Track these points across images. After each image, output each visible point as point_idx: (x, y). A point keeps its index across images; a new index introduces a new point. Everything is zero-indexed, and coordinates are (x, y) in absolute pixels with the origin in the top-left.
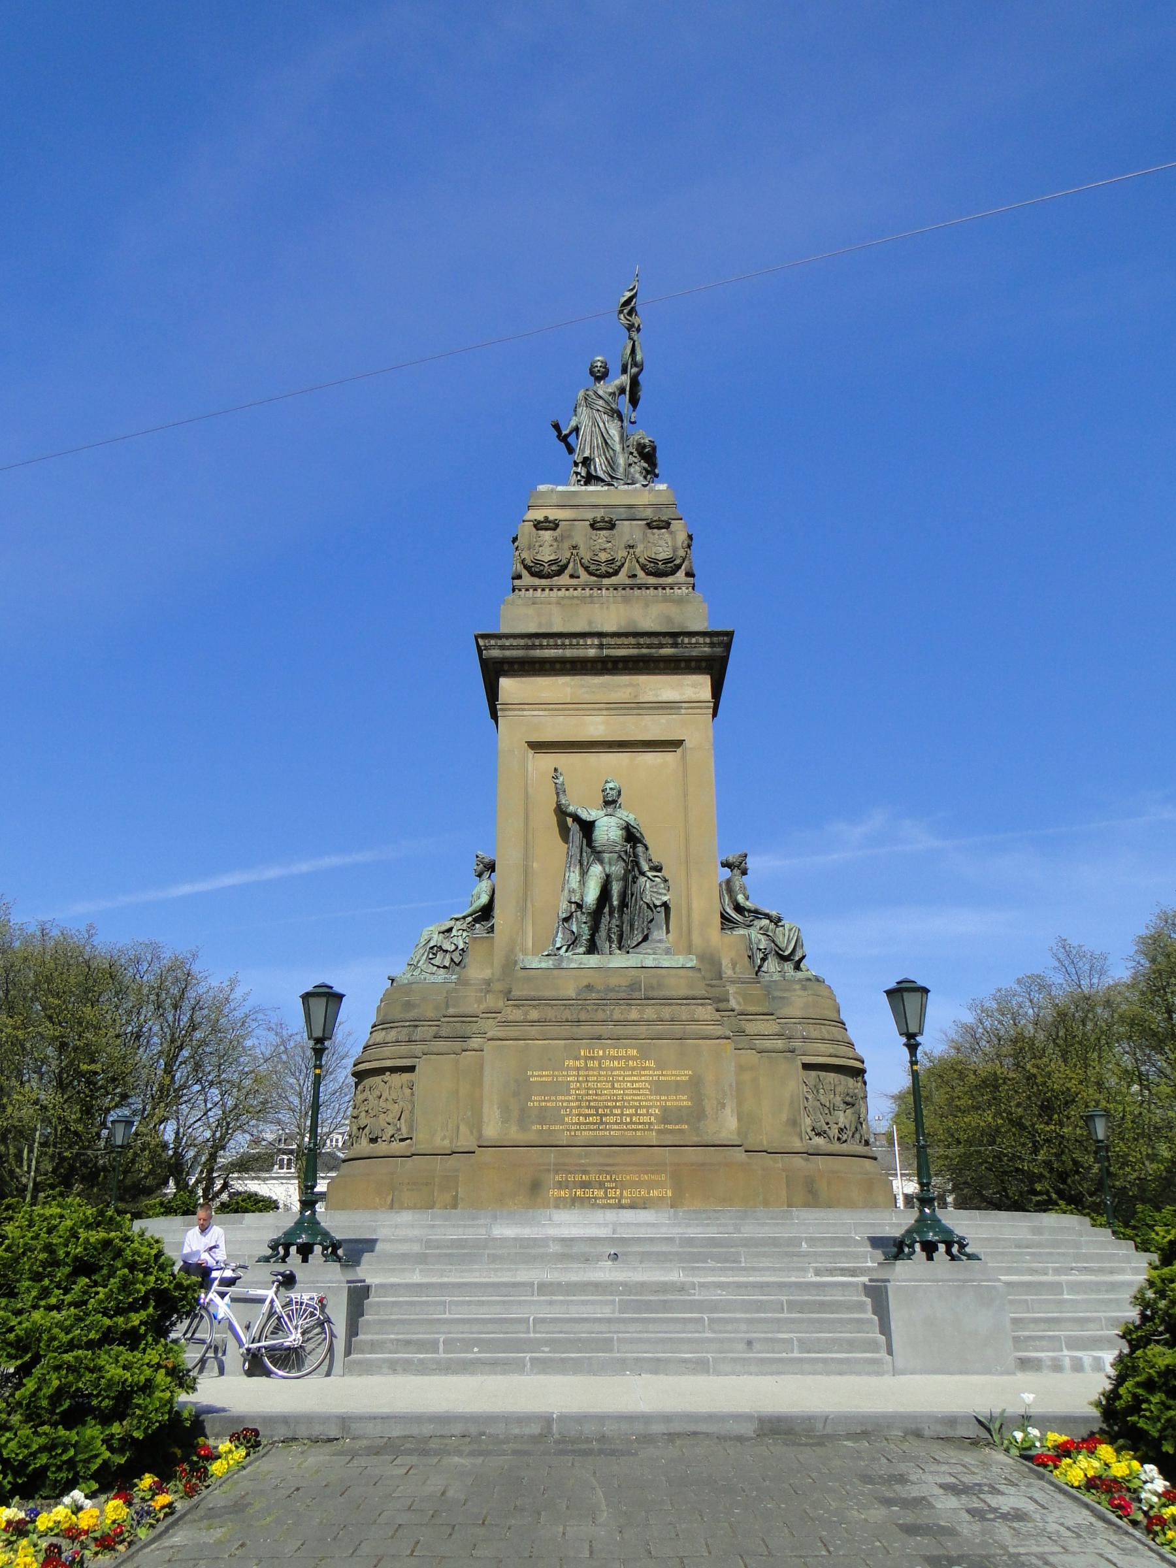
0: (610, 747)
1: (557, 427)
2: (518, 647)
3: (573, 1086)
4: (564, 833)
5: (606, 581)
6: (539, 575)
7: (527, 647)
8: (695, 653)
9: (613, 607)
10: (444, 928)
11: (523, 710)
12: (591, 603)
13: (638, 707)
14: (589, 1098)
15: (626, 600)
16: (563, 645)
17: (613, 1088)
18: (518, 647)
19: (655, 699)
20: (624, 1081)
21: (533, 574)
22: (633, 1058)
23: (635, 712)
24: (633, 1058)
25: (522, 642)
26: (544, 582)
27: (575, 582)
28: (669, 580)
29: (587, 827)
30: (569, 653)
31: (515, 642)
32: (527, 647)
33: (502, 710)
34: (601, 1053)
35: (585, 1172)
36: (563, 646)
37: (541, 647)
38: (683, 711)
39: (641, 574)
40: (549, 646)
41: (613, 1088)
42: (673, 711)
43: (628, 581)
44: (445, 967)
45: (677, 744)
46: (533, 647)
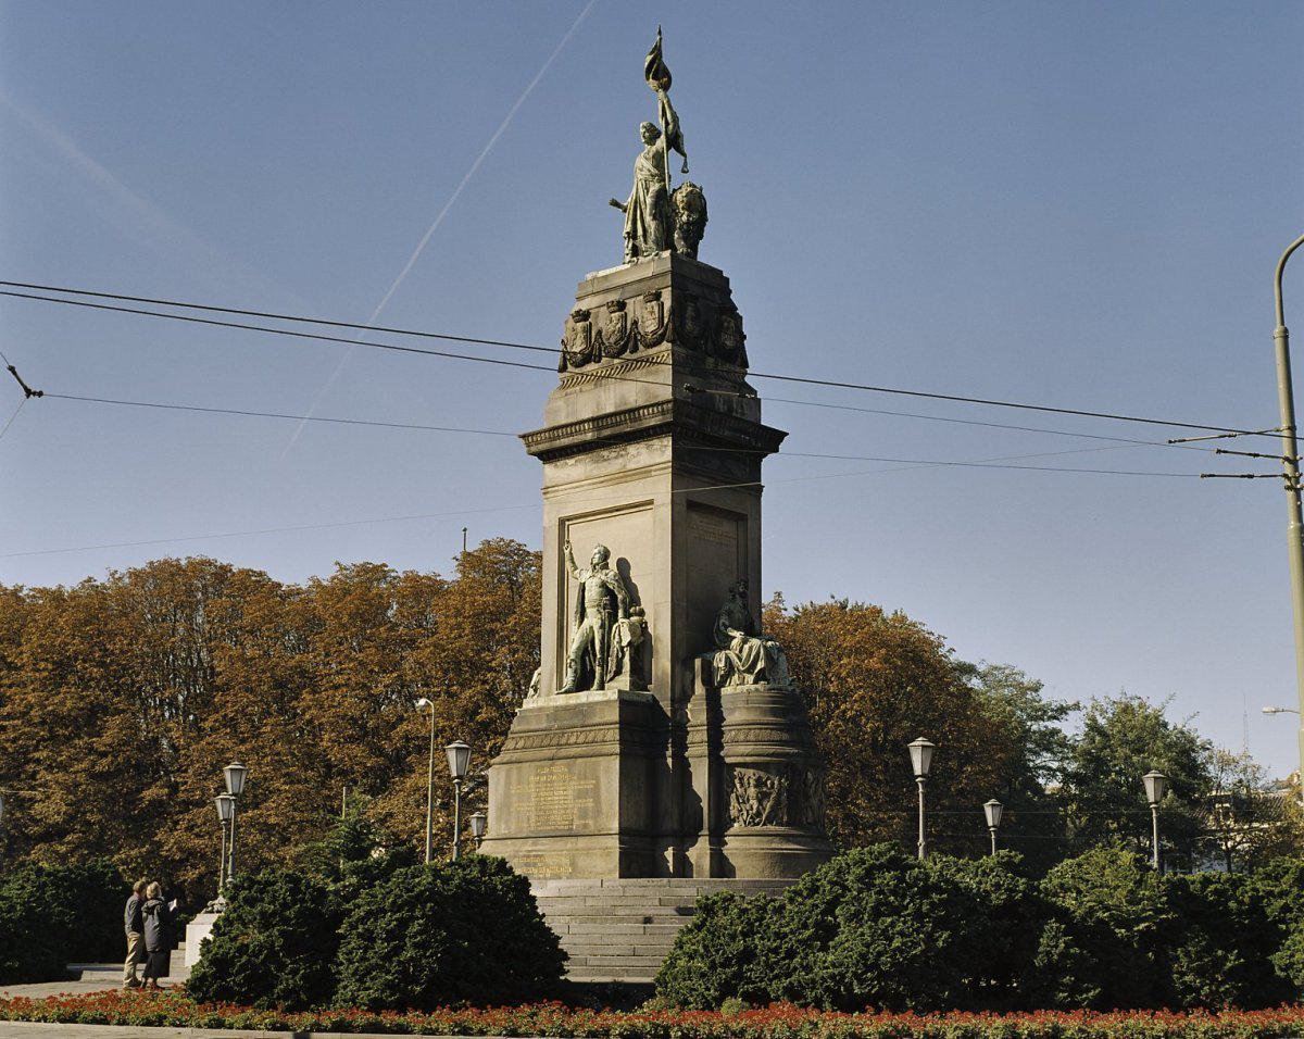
1: (615, 204)
8: (653, 422)
11: (557, 491)
13: (626, 476)
23: (623, 480)
35: (528, 857)
36: (572, 434)
37: (559, 437)
38: (653, 473)
46: (554, 439)
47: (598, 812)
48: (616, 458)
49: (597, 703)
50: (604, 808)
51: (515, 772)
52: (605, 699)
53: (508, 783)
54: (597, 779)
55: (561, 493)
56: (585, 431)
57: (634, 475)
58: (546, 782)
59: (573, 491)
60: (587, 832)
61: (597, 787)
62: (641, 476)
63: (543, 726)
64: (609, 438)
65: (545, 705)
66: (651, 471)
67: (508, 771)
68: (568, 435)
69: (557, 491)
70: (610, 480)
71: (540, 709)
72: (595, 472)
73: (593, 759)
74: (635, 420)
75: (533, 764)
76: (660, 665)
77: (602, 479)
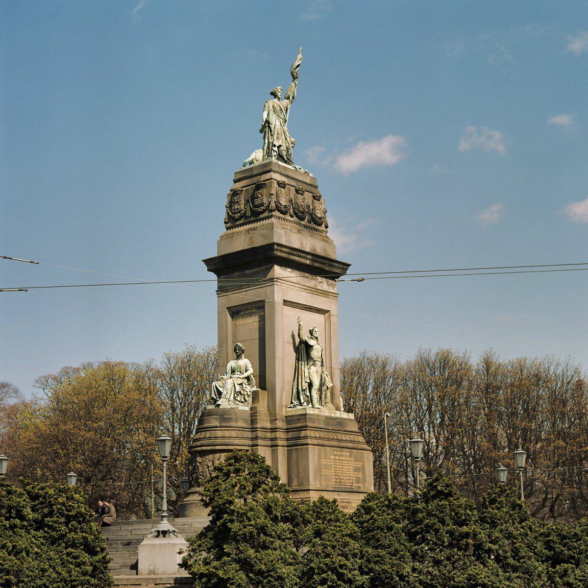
2: (286, 253)
4: (297, 350)
10: (239, 383)
11: (283, 283)
18: (286, 253)
22: (347, 456)
23: (316, 293)
24: (347, 456)
26: (282, 216)
27: (292, 219)
29: (309, 347)
32: (289, 254)
33: (276, 281)
36: (300, 256)
37: (293, 255)
43: (308, 224)
44: (243, 402)
47: (364, 480)
48: (312, 279)
49: (346, 419)
50: (367, 478)
51: (323, 452)
53: (320, 457)
54: (363, 462)
55: (284, 285)
56: (307, 259)
57: (321, 293)
60: (359, 490)
61: (363, 466)
62: (324, 295)
63: (322, 426)
64: (316, 268)
66: (329, 295)
68: (298, 256)
69: (283, 283)
70: (309, 290)
71: (318, 415)
73: (361, 451)
75: (333, 448)
76: (336, 402)
77: (306, 288)
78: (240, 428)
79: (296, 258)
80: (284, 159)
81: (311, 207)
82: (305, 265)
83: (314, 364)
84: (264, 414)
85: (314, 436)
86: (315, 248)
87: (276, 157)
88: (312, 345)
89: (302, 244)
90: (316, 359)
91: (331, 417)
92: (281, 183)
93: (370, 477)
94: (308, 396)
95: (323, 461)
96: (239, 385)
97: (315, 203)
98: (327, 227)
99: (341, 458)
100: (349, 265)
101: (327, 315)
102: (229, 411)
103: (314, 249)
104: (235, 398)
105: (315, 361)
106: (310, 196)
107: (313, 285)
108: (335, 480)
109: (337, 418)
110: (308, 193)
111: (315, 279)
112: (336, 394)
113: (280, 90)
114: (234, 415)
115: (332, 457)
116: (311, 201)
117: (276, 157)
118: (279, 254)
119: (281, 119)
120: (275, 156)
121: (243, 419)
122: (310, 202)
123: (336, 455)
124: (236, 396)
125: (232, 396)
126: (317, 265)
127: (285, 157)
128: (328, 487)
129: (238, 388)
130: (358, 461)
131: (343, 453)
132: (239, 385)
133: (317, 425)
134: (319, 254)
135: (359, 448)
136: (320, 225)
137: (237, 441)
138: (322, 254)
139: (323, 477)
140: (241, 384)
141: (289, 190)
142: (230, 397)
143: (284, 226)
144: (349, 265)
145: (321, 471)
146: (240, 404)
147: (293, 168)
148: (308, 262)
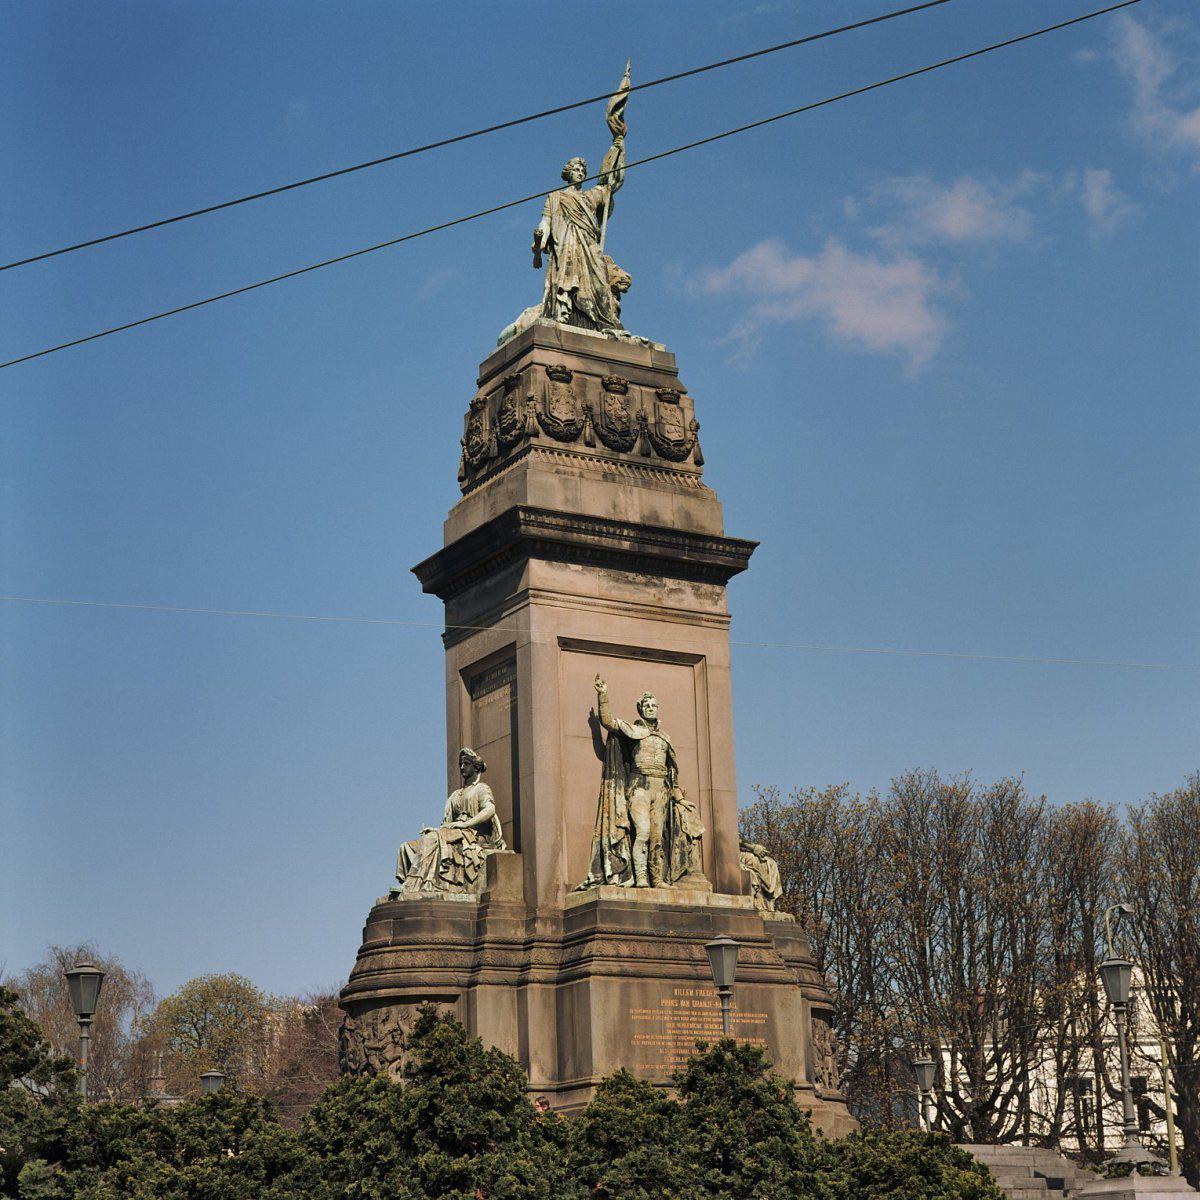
0: (634, 654)
2: (555, 527)
3: (668, 1025)
4: (601, 751)
5: (623, 456)
6: (558, 437)
7: (565, 528)
9: (635, 490)
10: (453, 838)
11: (554, 599)
12: (614, 481)
13: (664, 614)
14: (683, 1038)
15: (647, 484)
16: (614, 534)
17: (703, 1029)
18: (555, 527)
19: (678, 607)
20: (711, 1023)
21: (548, 433)
23: (659, 617)
25: (561, 522)
26: (561, 445)
27: (591, 451)
28: (675, 465)
29: (629, 746)
30: (606, 542)
31: (554, 521)
32: (565, 528)
33: (534, 596)
34: (692, 992)
36: (600, 534)
37: (579, 531)
39: (654, 454)
40: (586, 532)
41: (703, 1029)
42: (694, 622)
43: (642, 460)
44: (460, 884)
45: (699, 658)
46: (571, 530)
48: (646, 585)
49: (725, 910)
52: (735, 906)
53: (625, 1004)
54: (771, 1014)
55: (558, 603)
56: (621, 537)
57: (676, 616)
58: (691, 1009)
59: (580, 606)
61: (770, 1023)
62: (686, 621)
63: (647, 928)
64: (652, 557)
65: (639, 899)
66: (702, 619)
67: (625, 989)
68: (594, 533)
69: (554, 599)
70: (642, 611)
71: (634, 904)
72: (615, 594)
73: (760, 986)
74: (696, 549)
77: (627, 606)
78: (440, 944)
79: (589, 538)
80: (589, 319)
81: (651, 420)
82: (611, 552)
83: (643, 784)
84: (512, 908)
85: (614, 953)
86: (656, 512)
87: (567, 316)
88: (636, 736)
89: (615, 507)
90: (646, 772)
91: (676, 907)
92: (556, 371)
93: (794, 1051)
94: (624, 860)
95: (637, 1014)
96: (452, 843)
97: (662, 409)
98: (699, 462)
99: (696, 1004)
100: (753, 545)
101: (698, 666)
102: (416, 907)
103: (655, 515)
104: (439, 876)
105: (645, 775)
106: (648, 393)
107: (651, 598)
108: (678, 1059)
109: (697, 908)
110: (643, 388)
111: (655, 585)
112: (725, 852)
113: (576, 166)
114: (427, 914)
115: (668, 1003)
116: (651, 407)
117: (567, 316)
118: (534, 531)
119: (579, 231)
120: (564, 313)
121: (454, 924)
122: (649, 407)
123: (679, 998)
124: (441, 869)
125: (433, 870)
126: (655, 550)
127: (591, 314)
128: (653, 1076)
129: (447, 852)
130: (752, 1010)
131: (701, 993)
132: (452, 843)
133: (629, 927)
134: (670, 525)
135: (756, 977)
136: (681, 458)
137: (426, 976)
138: (678, 525)
139: (638, 1051)
140: (459, 842)
141: (583, 385)
142: (426, 874)
143: (561, 468)
144: (753, 545)
145: (630, 1038)
146: (454, 888)
147: (605, 337)
148: (626, 545)
